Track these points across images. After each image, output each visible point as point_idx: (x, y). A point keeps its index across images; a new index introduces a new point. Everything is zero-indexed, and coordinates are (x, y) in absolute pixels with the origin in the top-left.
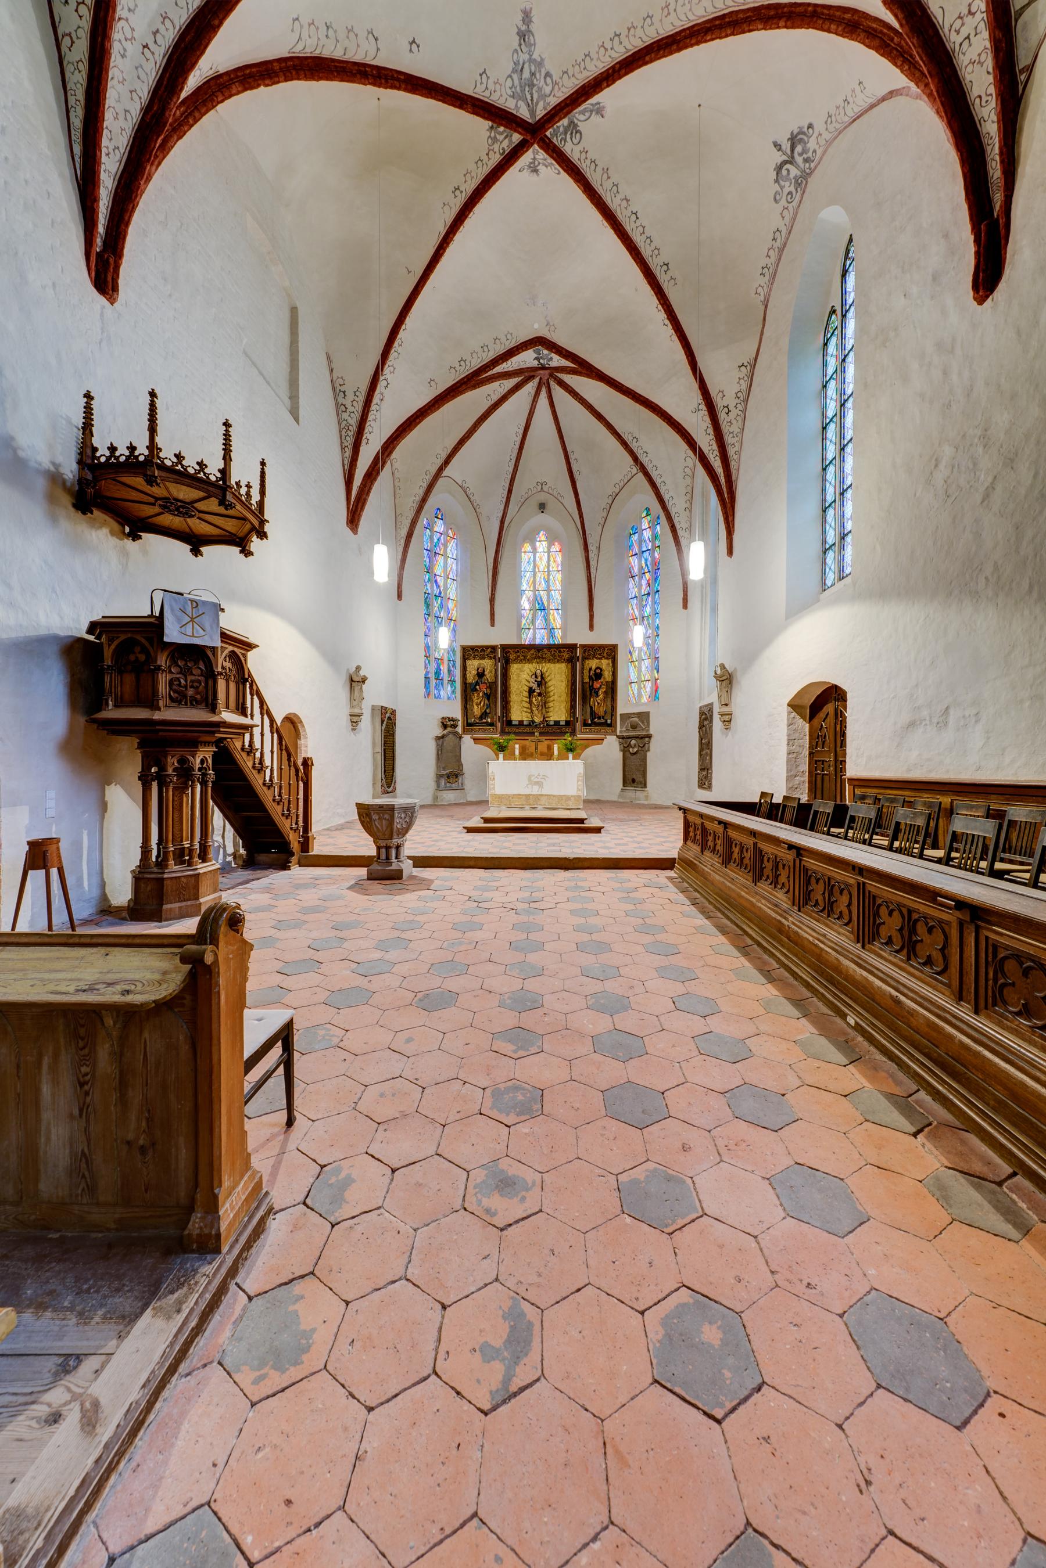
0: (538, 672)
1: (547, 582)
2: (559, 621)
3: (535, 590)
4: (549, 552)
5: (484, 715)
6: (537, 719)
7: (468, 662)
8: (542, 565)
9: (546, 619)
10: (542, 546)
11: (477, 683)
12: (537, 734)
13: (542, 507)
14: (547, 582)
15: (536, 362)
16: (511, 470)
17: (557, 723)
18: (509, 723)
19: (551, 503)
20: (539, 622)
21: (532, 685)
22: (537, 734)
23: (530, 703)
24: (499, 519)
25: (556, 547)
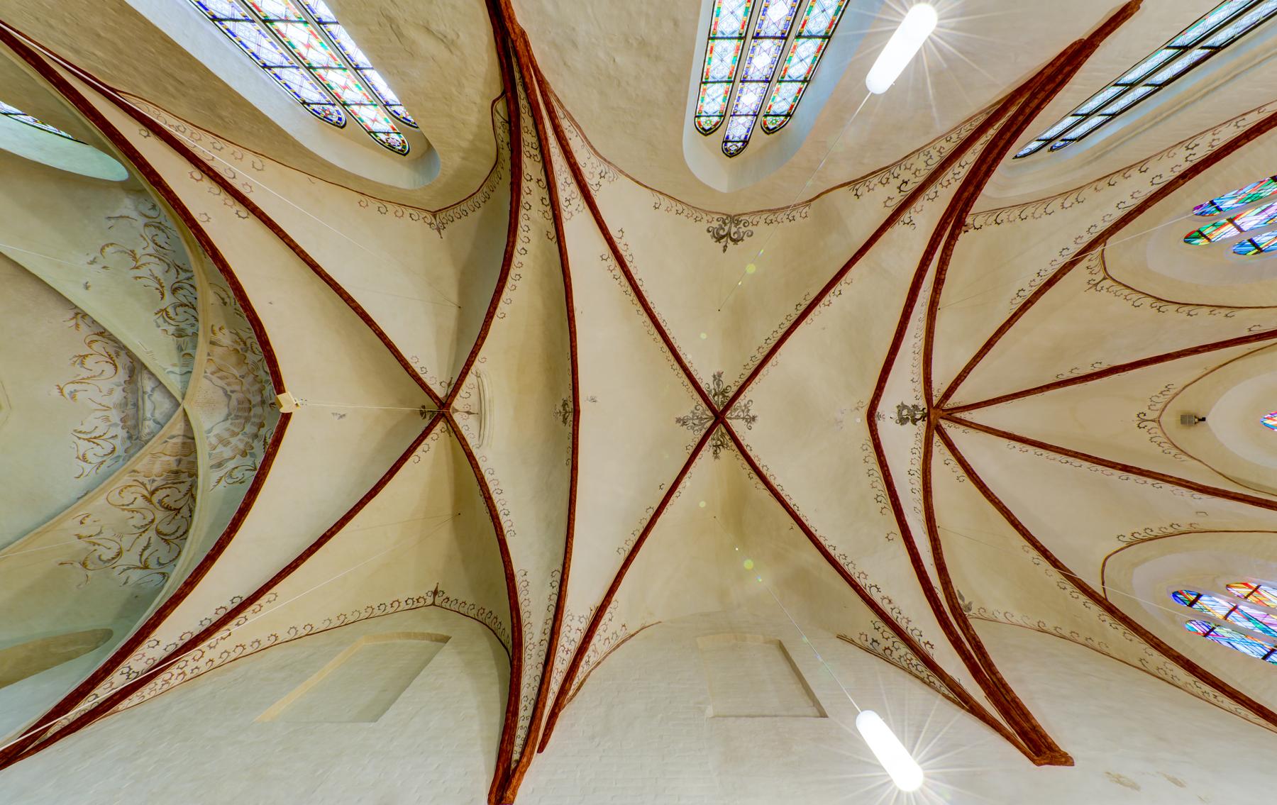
13: (1193, 420)
15: (920, 423)
16: (1087, 464)
19: (1188, 403)
24: (1197, 495)
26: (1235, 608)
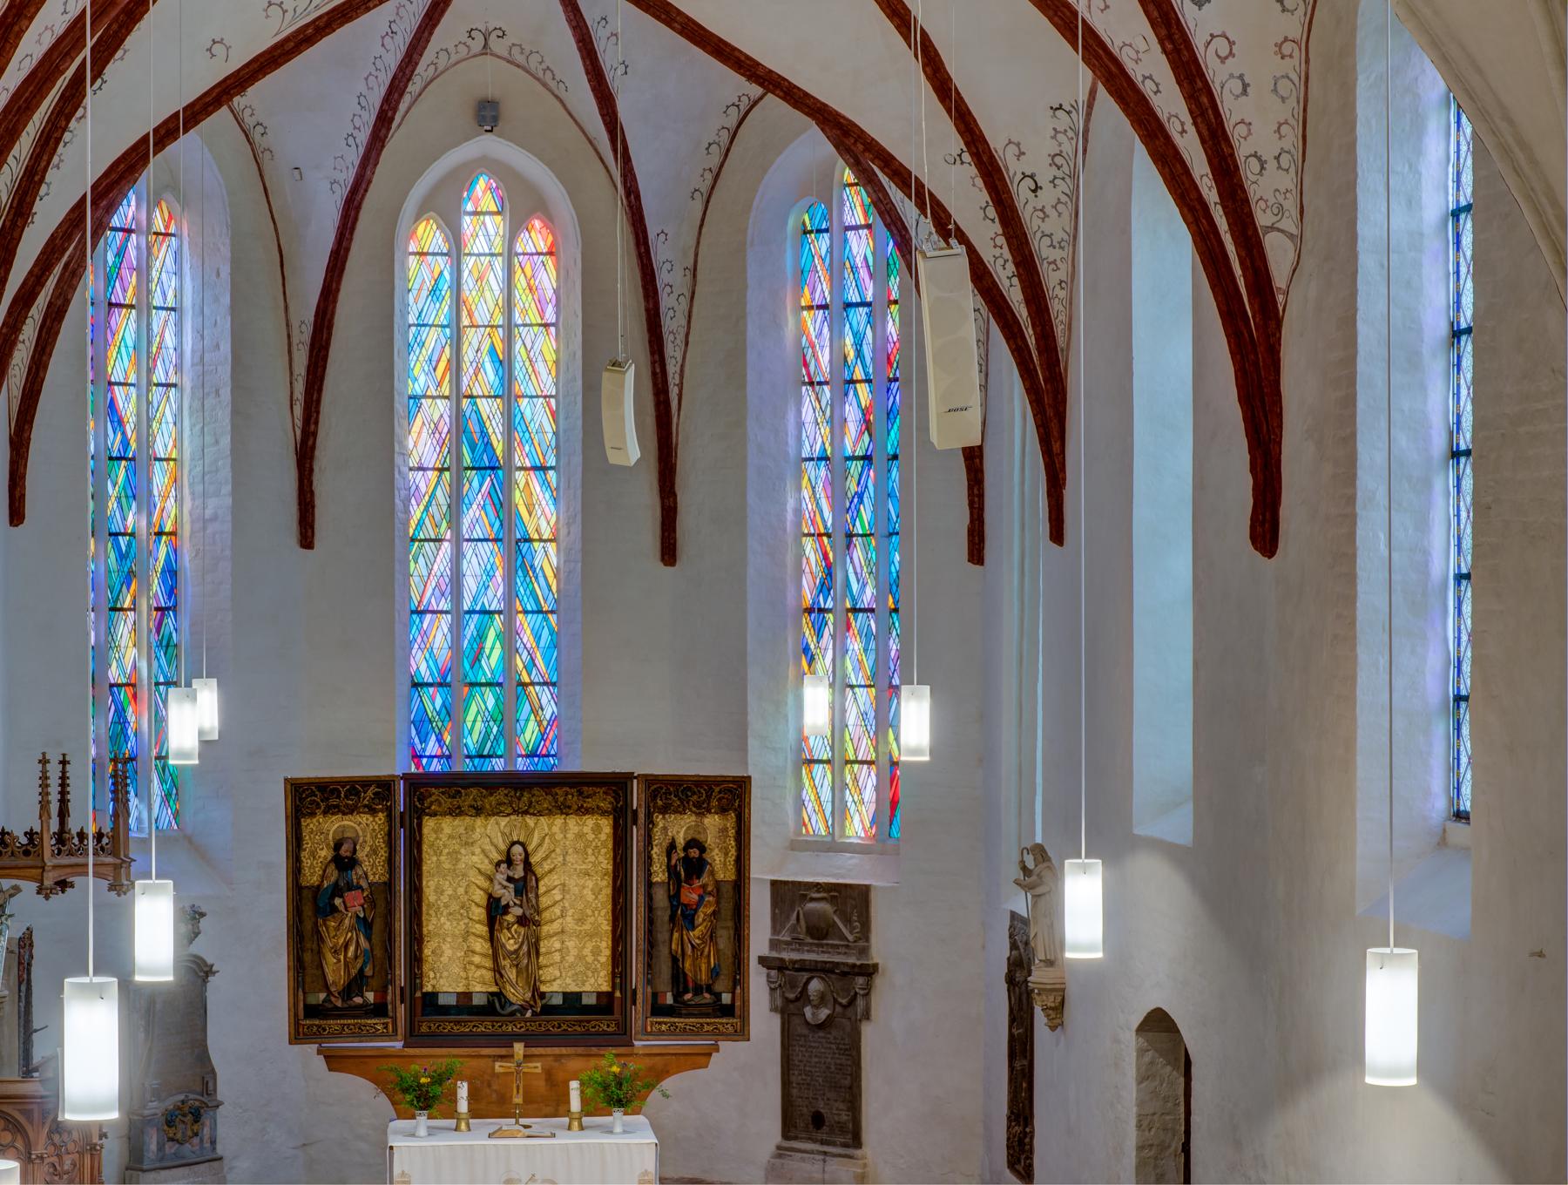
1: (505, 364)
2: (550, 509)
3: (458, 395)
4: (510, 254)
8: (484, 303)
9: (502, 505)
13: (488, 115)
14: (505, 364)
20: (477, 518)
25: (535, 239)
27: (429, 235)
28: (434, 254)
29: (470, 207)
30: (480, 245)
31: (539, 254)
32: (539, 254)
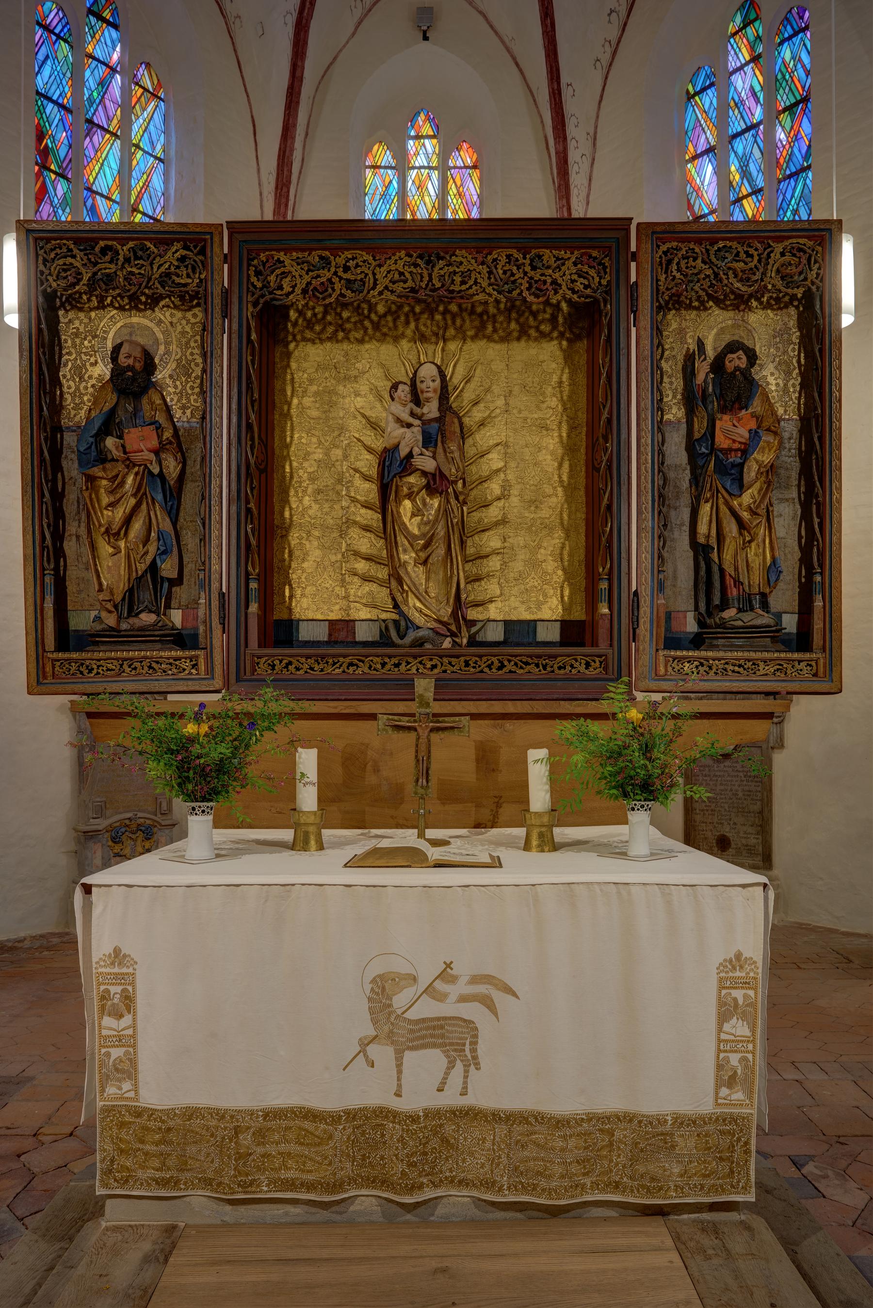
0: (428, 371)
4: (444, 168)
5: (152, 585)
6: (425, 609)
7: (72, 323)
10: (423, 152)
11: (109, 425)
12: (424, 686)
17: (519, 632)
18: (281, 632)
21: (396, 432)
22: (424, 686)
23: (388, 528)
25: (464, 157)
26: (113, 70)
27: (383, 155)
28: (386, 167)
29: (413, 133)
30: (421, 161)
31: (466, 167)
32: (466, 167)
